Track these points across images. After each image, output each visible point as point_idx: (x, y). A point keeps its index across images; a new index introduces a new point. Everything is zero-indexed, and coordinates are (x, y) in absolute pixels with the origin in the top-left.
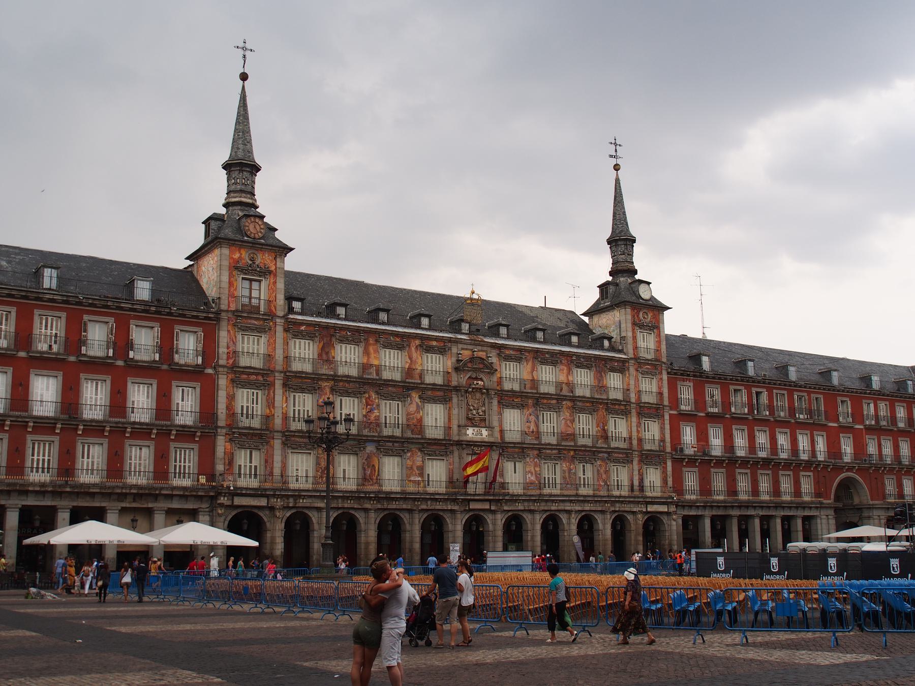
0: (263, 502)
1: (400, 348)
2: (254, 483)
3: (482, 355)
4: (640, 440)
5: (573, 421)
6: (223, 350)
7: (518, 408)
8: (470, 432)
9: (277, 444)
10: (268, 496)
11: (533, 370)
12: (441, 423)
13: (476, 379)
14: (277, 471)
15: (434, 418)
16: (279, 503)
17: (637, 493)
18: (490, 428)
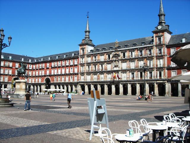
0: (83, 84)
1: (103, 55)
2: (83, 81)
3: (118, 53)
4: (157, 65)
5: (138, 63)
6: (80, 61)
7: (125, 62)
8: (115, 69)
9: (86, 74)
10: (84, 83)
11: (129, 53)
12: (110, 67)
13: (116, 58)
14: (86, 79)
15: (109, 67)
16: (85, 84)
17: (155, 78)
18: (119, 67)
